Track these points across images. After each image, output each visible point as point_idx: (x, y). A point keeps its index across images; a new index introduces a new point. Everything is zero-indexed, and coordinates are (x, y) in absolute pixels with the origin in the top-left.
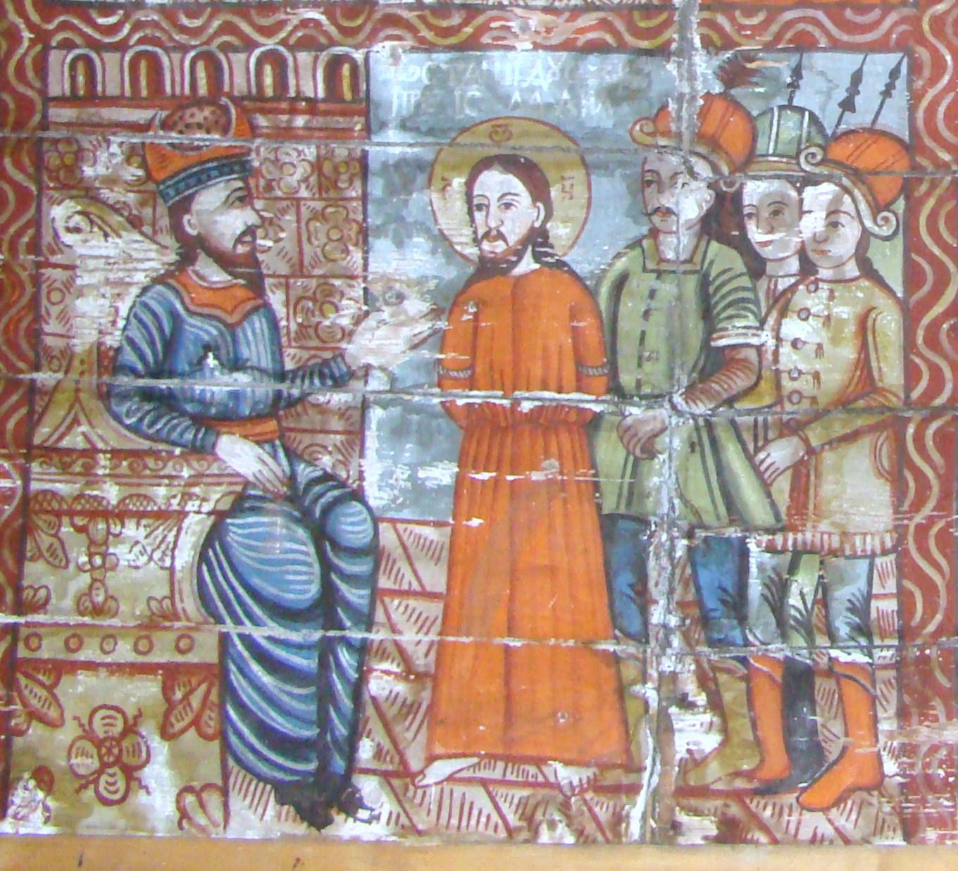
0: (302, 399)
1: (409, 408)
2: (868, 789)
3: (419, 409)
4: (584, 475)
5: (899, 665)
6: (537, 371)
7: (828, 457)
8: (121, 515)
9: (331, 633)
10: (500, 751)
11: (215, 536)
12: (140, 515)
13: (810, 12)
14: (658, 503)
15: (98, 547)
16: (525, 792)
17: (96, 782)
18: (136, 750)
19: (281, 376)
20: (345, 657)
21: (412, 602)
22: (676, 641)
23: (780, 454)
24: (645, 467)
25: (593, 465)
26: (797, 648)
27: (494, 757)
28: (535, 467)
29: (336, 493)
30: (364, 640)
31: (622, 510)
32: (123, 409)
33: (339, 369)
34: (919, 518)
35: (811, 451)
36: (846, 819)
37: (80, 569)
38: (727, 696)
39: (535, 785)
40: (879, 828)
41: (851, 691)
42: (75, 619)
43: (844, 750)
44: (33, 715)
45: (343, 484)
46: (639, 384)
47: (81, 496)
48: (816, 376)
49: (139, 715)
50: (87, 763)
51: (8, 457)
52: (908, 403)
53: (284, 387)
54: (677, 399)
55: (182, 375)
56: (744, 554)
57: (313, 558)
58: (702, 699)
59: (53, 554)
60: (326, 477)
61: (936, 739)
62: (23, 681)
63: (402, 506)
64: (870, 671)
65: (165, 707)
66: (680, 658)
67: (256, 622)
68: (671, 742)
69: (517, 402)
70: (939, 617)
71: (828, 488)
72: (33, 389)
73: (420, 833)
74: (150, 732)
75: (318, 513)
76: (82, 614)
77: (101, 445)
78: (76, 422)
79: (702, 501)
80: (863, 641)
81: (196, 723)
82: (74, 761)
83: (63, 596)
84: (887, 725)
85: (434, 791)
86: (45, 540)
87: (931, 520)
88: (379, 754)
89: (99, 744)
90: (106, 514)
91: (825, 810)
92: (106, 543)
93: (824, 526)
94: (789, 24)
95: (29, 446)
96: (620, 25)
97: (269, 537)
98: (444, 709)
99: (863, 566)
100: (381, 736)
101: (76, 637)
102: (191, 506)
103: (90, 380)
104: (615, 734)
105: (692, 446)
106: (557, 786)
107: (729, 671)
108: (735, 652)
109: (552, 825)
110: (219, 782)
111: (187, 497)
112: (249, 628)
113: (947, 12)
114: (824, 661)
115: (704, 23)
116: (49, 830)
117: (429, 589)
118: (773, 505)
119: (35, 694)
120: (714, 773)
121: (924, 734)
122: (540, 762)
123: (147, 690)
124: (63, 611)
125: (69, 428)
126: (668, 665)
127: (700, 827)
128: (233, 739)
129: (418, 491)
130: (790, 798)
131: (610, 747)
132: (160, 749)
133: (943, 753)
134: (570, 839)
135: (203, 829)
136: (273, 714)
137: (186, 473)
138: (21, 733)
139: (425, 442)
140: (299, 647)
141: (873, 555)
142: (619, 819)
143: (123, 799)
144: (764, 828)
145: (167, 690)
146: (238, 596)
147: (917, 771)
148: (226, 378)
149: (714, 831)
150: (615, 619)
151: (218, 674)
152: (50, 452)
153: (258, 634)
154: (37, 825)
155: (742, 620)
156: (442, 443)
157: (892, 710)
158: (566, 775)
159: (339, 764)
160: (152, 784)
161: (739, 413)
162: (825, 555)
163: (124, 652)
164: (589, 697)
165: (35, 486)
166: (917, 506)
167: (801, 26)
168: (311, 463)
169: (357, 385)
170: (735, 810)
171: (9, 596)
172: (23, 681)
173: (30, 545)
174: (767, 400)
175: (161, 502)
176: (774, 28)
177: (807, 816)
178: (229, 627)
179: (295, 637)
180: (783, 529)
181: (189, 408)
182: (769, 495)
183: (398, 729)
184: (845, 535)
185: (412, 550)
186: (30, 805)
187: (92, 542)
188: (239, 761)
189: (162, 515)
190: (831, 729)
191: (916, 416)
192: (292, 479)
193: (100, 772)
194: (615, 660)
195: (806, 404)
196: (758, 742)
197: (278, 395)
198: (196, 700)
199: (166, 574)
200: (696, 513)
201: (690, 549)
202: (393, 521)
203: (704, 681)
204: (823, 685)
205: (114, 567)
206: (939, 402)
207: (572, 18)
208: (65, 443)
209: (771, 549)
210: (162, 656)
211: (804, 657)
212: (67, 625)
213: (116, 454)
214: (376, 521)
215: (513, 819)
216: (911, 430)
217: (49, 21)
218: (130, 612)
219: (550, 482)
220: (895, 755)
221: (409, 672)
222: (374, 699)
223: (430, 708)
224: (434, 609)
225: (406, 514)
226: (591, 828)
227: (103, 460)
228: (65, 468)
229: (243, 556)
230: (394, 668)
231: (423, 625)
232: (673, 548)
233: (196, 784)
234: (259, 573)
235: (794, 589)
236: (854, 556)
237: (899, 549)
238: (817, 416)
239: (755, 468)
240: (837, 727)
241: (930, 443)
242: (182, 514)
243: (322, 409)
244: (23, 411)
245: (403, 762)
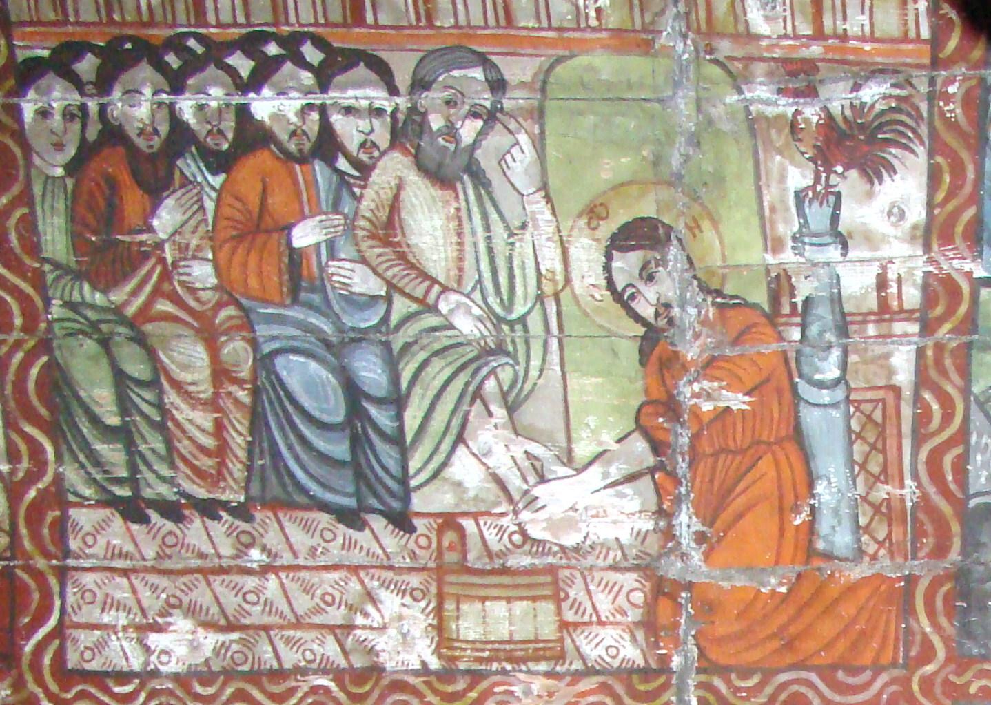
13: (804, 675)
94: (783, 686)
96: (620, 689)
113: (936, 673)
115: (700, 686)
167: (795, 688)
176: (769, 690)
207: (572, 683)
217: (67, 690)
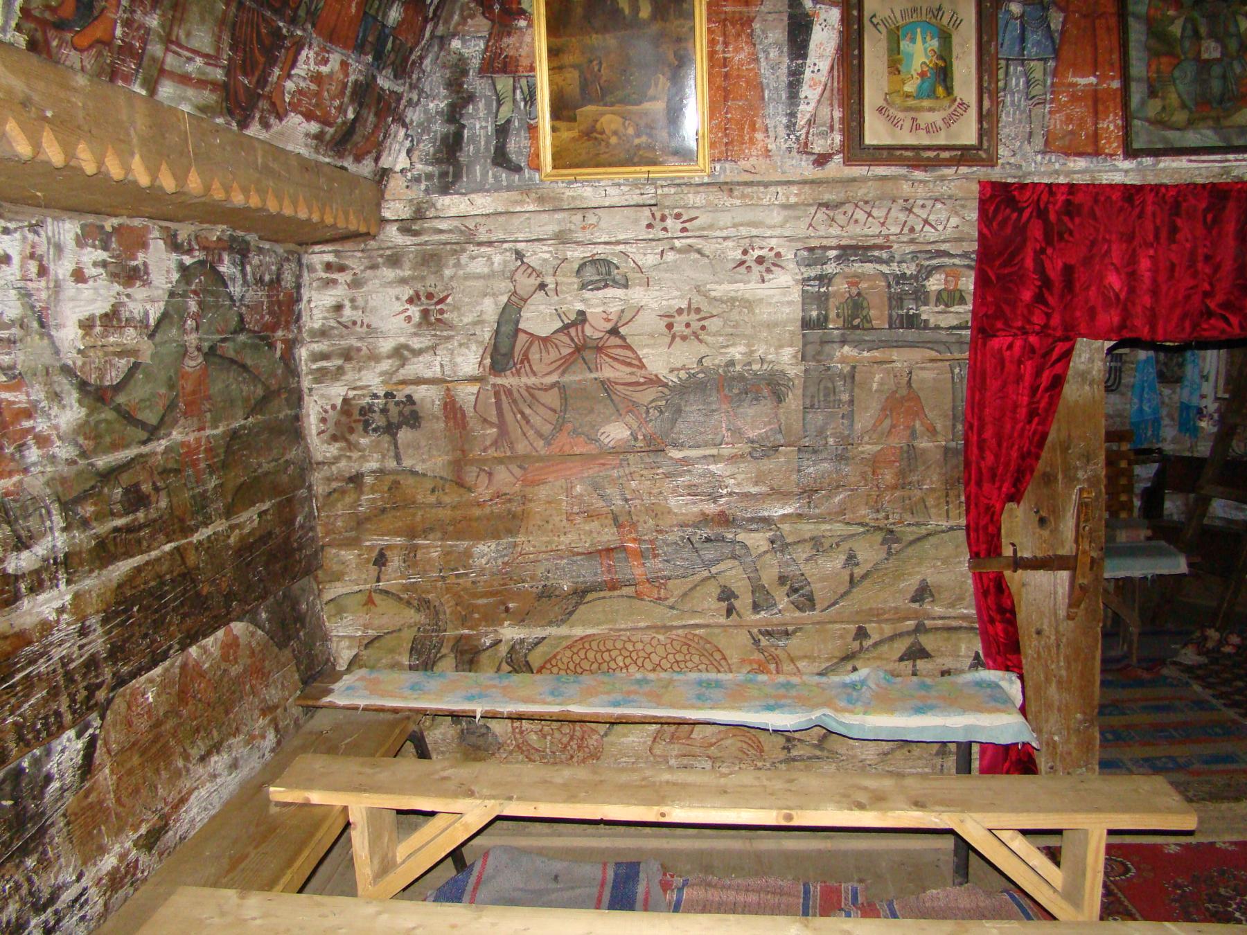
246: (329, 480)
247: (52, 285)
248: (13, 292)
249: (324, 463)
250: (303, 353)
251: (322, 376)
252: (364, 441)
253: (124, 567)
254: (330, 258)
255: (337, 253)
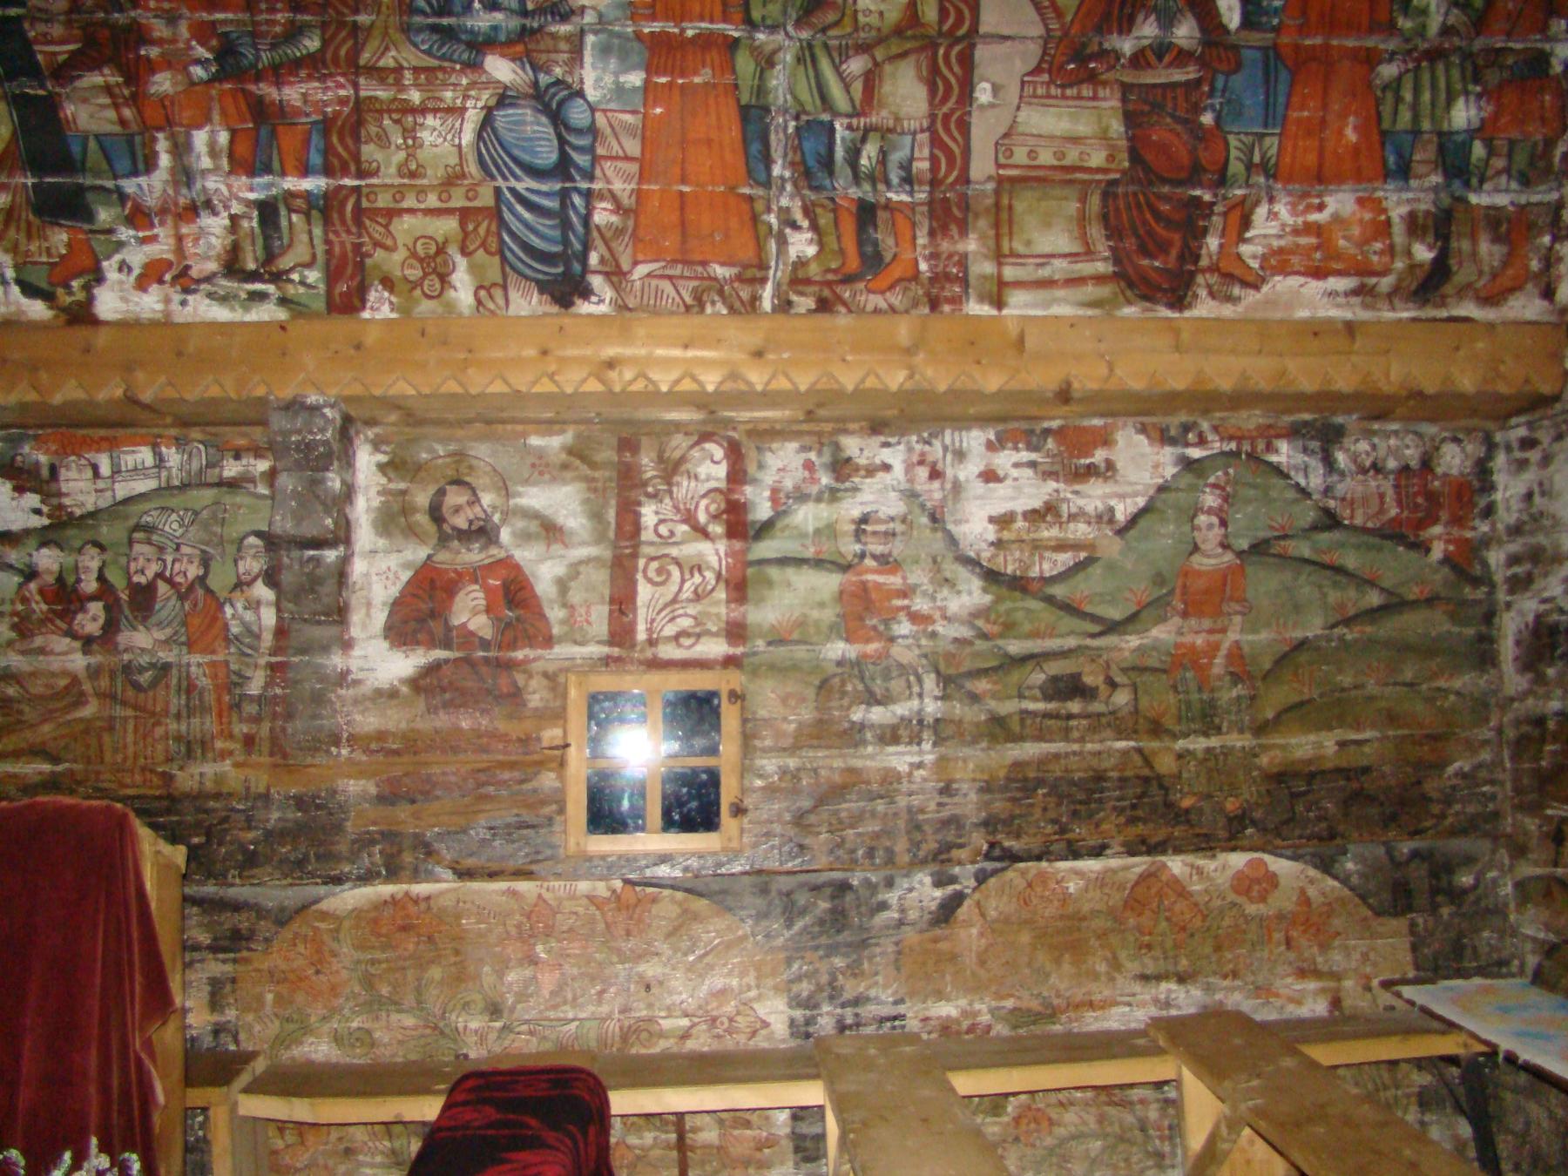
0: (541, 28)
1: (612, 34)
2: (909, 280)
3: (619, 35)
4: (728, 79)
5: (931, 203)
6: (697, 8)
7: (888, 68)
8: (423, 110)
9: (568, 185)
10: (679, 257)
11: (487, 122)
12: (435, 111)
14: (776, 98)
15: (410, 133)
16: (695, 283)
17: (421, 285)
18: (445, 263)
19: (525, 13)
20: (577, 200)
21: (620, 164)
22: (789, 187)
23: (856, 65)
24: (767, 74)
25: (734, 72)
26: (865, 191)
27: (675, 261)
28: (696, 73)
29: (565, 93)
30: (589, 190)
31: (753, 101)
32: (418, 39)
33: (563, 9)
34: (945, 109)
35: (876, 64)
36: (896, 299)
37: (398, 147)
38: (822, 222)
39: (702, 278)
40: (915, 304)
41: (901, 222)
42: (397, 181)
43: (895, 256)
44: (377, 244)
45: (569, 87)
46: (763, 18)
47: (395, 99)
48: (881, 14)
49: (446, 242)
50: (415, 273)
51: (344, 75)
52: (940, 34)
53: (528, 22)
54: (790, 28)
55: (457, 15)
56: (832, 130)
57: (553, 136)
58: (806, 224)
59: (379, 138)
60: (558, 82)
61: (952, 249)
62: (367, 222)
63: (610, 100)
64: (912, 207)
65: (460, 237)
66: (792, 197)
67: (517, 178)
68: (787, 252)
69: (683, 31)
70: (955, 173)
71: (887, 88)
72: (355, 27)
73: (630, 310)
74: (453, 251)
75: (554, 106)
76: (402, 177)
77: (405, 64)
78: (387, 49)
79: (805, 96)
80: (907, 188)
81: (483, 245)
82: (407, 272)
83: (388, 165)
84: (922, 240)
85: (638, 284)
86: (373, 129)
87: (953, 111)
88: (602, 261)
89: (421, 260)
90: (413, 110)
91: (882, 292)
92: (414, 130)
93: (884, 113)
95: (357, 67)
97: (524, 123)
98: (641, 233)
99: (908, 139)
100: (602, 248)
101: (400, 193)
102: (469, 104)
103: (394, 20)
104: (751, 245)
105: (799, 60)
106: (716, 279)
107: (823, 206)
108: (825, 194)
109: (713, 303)
110: (500, 281)
111: (466, 97)
112: (513, 183)
114: (883, 200)
116: (394, 315)
117: (629, 153)
118: (852, 100)
119: (376, 231)
120: (814, 270)
121: (945, 246)
122: (704, 264)
123: (449, 225)
124: (389, 176)
125: (383, 54)
126: (784, 202)
127: (804, 303)
128: (508, 255)
129: (620, 90)
130: (861, 285)
131: (748, 254)
132: (462, 263)
133: (956, 258)
134: (725, 311)
135: (492, 312)
136: (533, 237)
137: (464, 81)
138: (370, 256)
139: (624, 56)
140: (547, 195)
141: (914, 134)
142: (755, 299)
143: (439, 296)
144: (845, 304)
145: (463, 225)
146: (506, 164)
147: (939, 269)
148: (487, 16)
149: (813, 306)
150: (749, 173)
151: (496, 214)
152: (373, 71)
153: (520, 186)
154: (386, 312)
155: (831, 174)
156: (635, 58)
157: (925, 230)
158: (720, 271)
159: (577, 267)
160: (458, 285)
161: (830, 38)
162: (885, 132)
163: (432, 201)
164: (734, 223)
165: (363, 94)
166: (945, 100)
168: (548, 72)
169: (575, 19)
170: (826, 293)
171: (353, 168)
172: (367, 222)
173: (363, 133)
174: (849, 30)
175: (449, 101)
177: (872, 297)
178: (500, 182)
179: (544, 188)
180: (858, 115)
181: (463, 37)
182: (848, 92)
183: (614, 245)
184: (897, 119)
185: (617, 129)
186: (381, 300)
187: (405, 130)
188: (513, 268)
189: (450, 110)
190: (887, 243)
191: (944, 42)
192: (536, 84)
193: (423, 278)
194: (750, 199)
195: (874, 33)
196: (842, 252)
197: (524, 27)
198: (482, 230)
199: (455, 150)
200: (802, 105)
201: (797, 129)
202: (605, 111)
203: (807, 211)
204: (882, 215)
205: (421, 146)
206: (961, 32)
208: (381, 63)
209: (849, 127)
210: (458, 202)
211: (870, 198)
212: (392, 186)
213: (416, 70)
214: (593, 109)
215: (689, 300)
216: (941, 51)
218: (434, 175)
219: (706, 84)
220: (928, 259)
221: (619, 208)
222: (598, 227)
223: (634, 230)
224: (634, 168)
225: (612, 106)
226: (737, 305)
227: (408, 74)
228: (382, 81)
229: (508, 137)
230: (609, 206)
231: (627, 178)
232: (786, 128)
233: (486, 284)
234: (517, 146)
235: (864, 154)
236: (903, 133)
237: (931, 129)
238: (881, 41)
239: (840, 74)
240: (890, 241)
241: (953, 60)
242: (463, 109)
243: (554, 36)
244: (350, 43)
245: (618, 266)
246: (1517, 723)
247: (948, 486)
248: (893, 495)
249: (1512, 700)
250: (1495, 557)
251: (1519, 584)
252: (1550, 672)
253: (1030, 750)
254: (1522, 432)
255: (1530, 425)
